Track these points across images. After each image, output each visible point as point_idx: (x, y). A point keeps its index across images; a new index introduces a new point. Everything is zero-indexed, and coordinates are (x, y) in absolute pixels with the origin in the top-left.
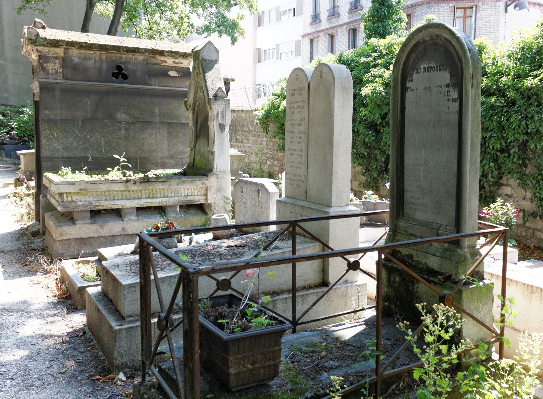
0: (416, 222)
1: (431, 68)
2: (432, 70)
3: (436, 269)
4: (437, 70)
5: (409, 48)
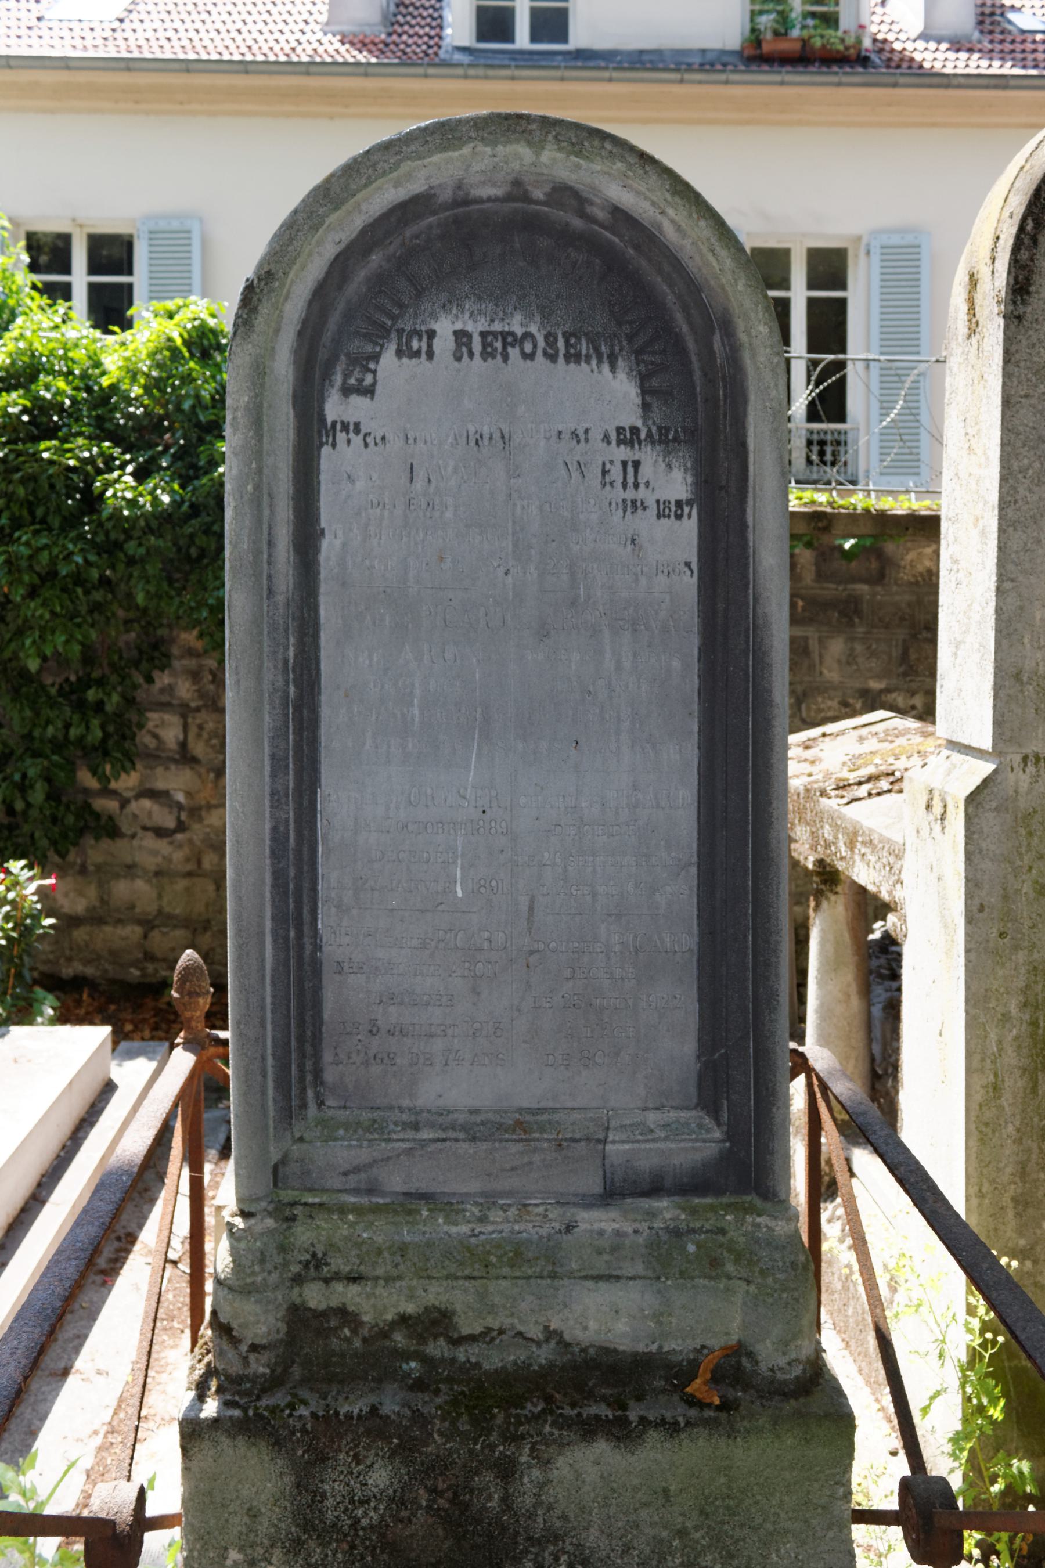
0: (432, 1125)
1: (509, 339)
2: (514, 353)
3: (625, 1345)
4: (553, 358)
5: (358, 222)
